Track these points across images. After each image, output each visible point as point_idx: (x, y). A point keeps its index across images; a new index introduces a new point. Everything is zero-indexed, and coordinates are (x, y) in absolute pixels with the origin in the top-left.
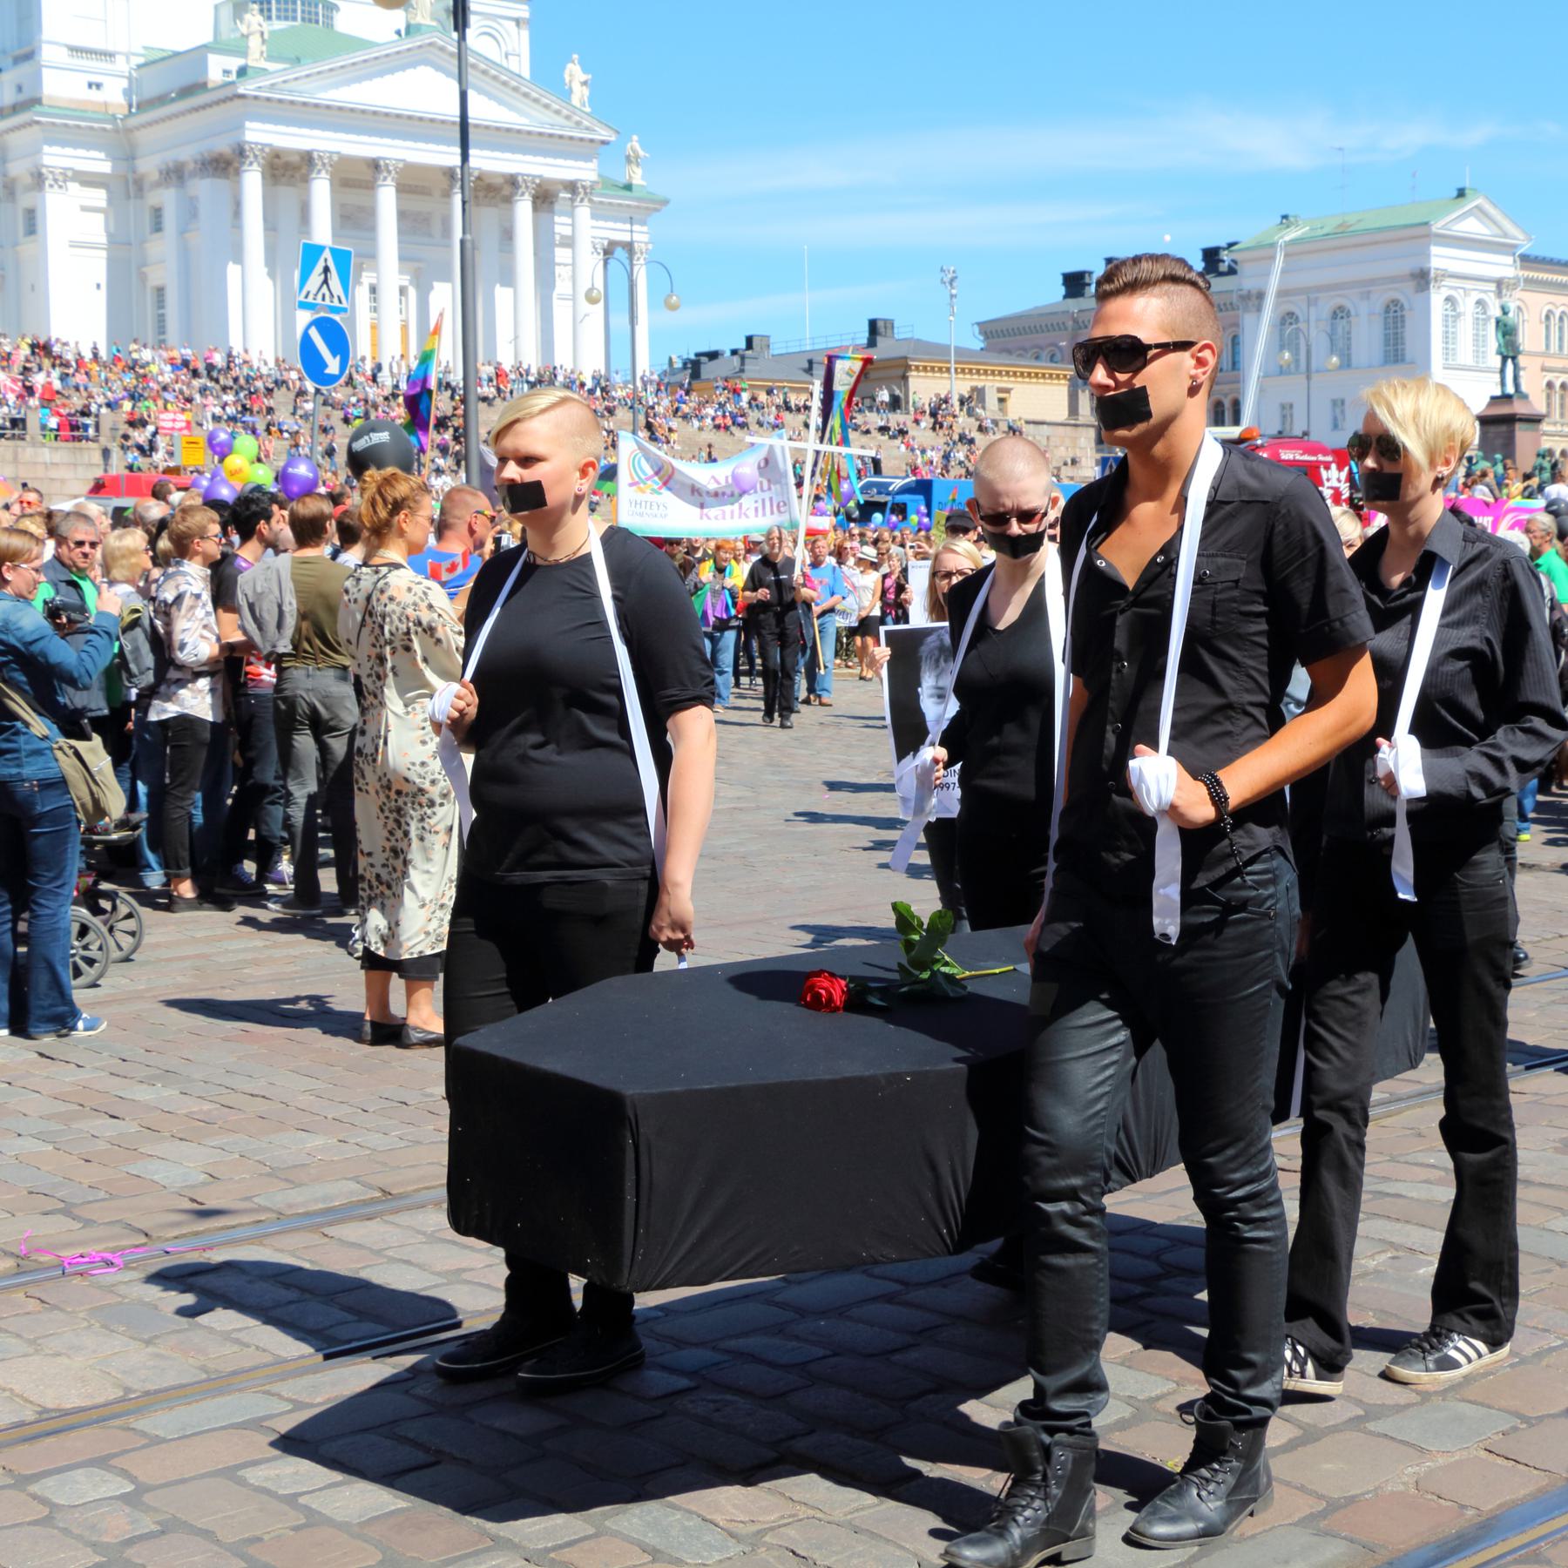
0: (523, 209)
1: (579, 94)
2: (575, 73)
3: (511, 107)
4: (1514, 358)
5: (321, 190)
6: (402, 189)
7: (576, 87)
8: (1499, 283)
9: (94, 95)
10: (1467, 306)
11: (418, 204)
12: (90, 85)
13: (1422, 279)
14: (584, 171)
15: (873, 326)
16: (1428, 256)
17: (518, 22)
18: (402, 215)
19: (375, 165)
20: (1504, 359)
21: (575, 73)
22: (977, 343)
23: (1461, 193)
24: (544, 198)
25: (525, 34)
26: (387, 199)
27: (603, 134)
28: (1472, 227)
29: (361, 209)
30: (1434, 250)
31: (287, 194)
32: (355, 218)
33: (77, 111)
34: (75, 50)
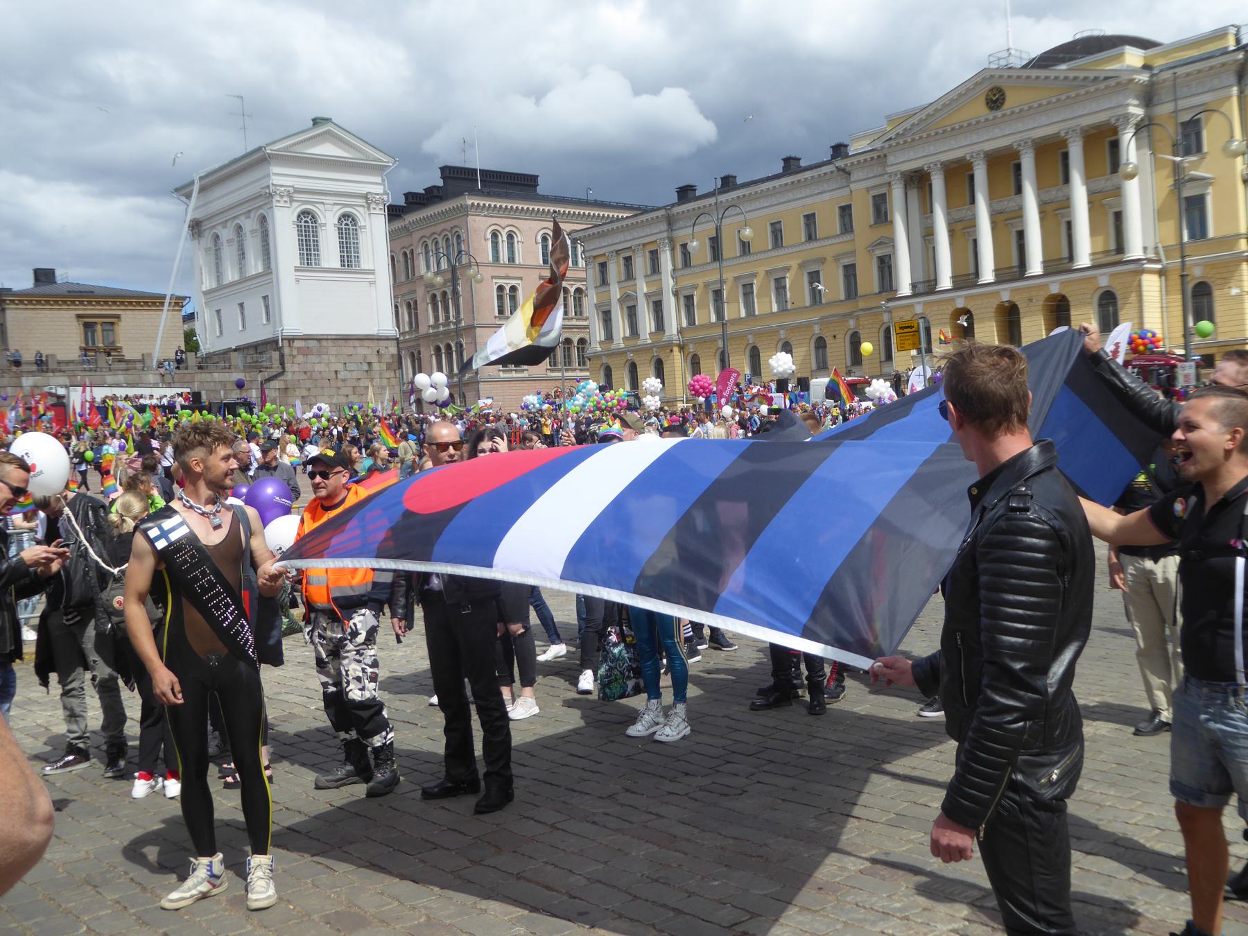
10: (328, 219)
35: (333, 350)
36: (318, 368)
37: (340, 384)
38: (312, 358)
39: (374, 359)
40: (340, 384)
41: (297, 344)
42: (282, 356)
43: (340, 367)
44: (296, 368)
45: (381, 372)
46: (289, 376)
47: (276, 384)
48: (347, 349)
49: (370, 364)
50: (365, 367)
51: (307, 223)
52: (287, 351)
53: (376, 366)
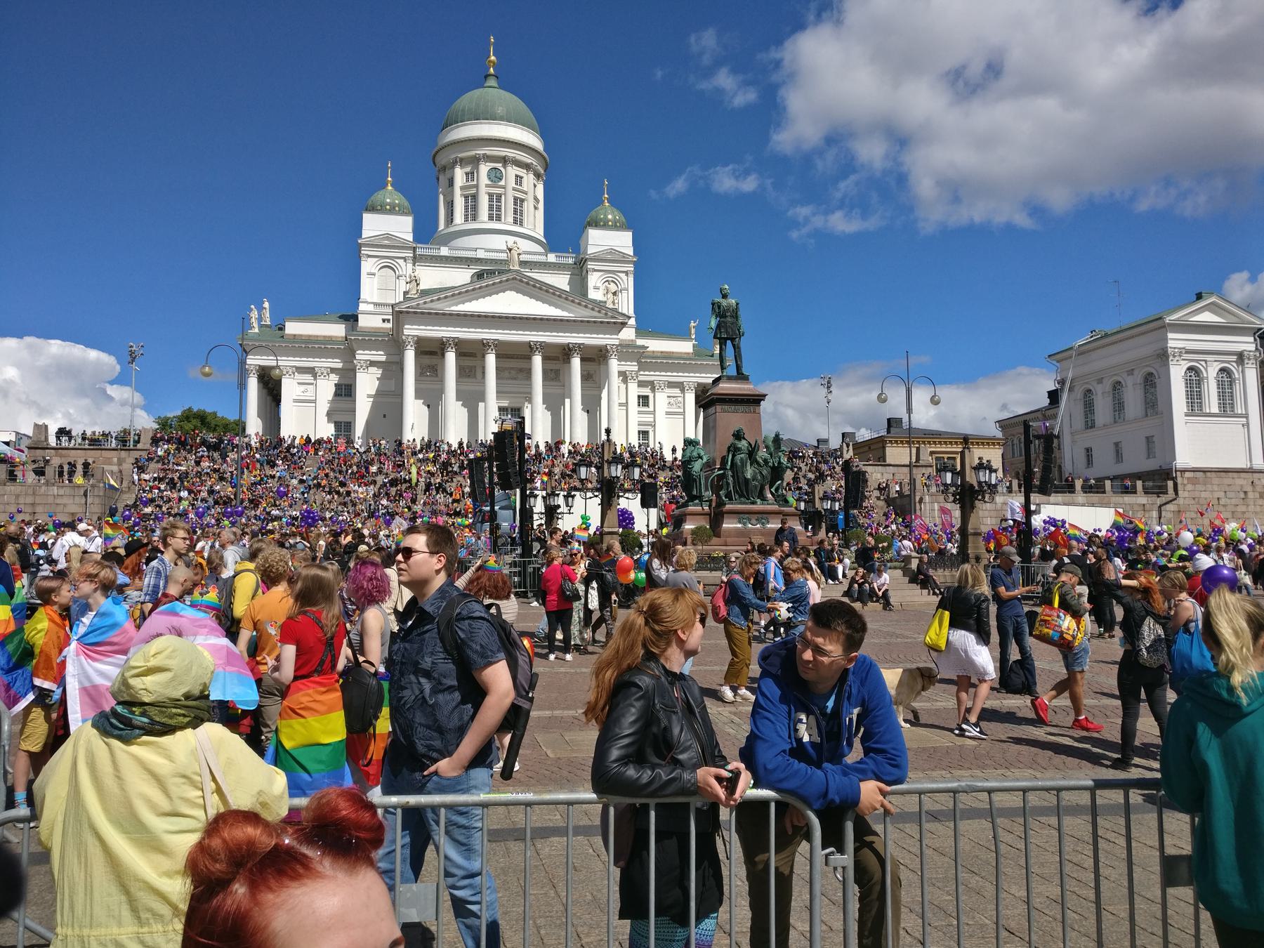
3: (557, 306)
4: (732, 340)
8: (1241, 357)
10: (1211, 373)
12: (384, 321)
13: (1163, 356)
15: (889, 420)
16: (1166, 340)
17: (626, 273)
20: (723, 343)
22: (999, 434)
23: (1199, 297)
25: (631, 279)
26: (491, 359)
28: (1207, 317)
30: (1170, 335)
34: (376, 304)
35: (1216, 481)
36: (1203, 495)
37: (1221, 508)
38: (1199, 487)
39: (1249, 488)
40: (1221, 508)
41: (1187, 475)
42: (1176, 485)
43: (1221, 495)
44: (1186, 494)
45: (1255, 499)
46: (1180, 501)
47: (1170, 507)
48: (1227, 480)
49: (1245, 493)
50: (1242, 495)
51: (1194, 377)
52: (1179, 480)
53: (1251, 495)
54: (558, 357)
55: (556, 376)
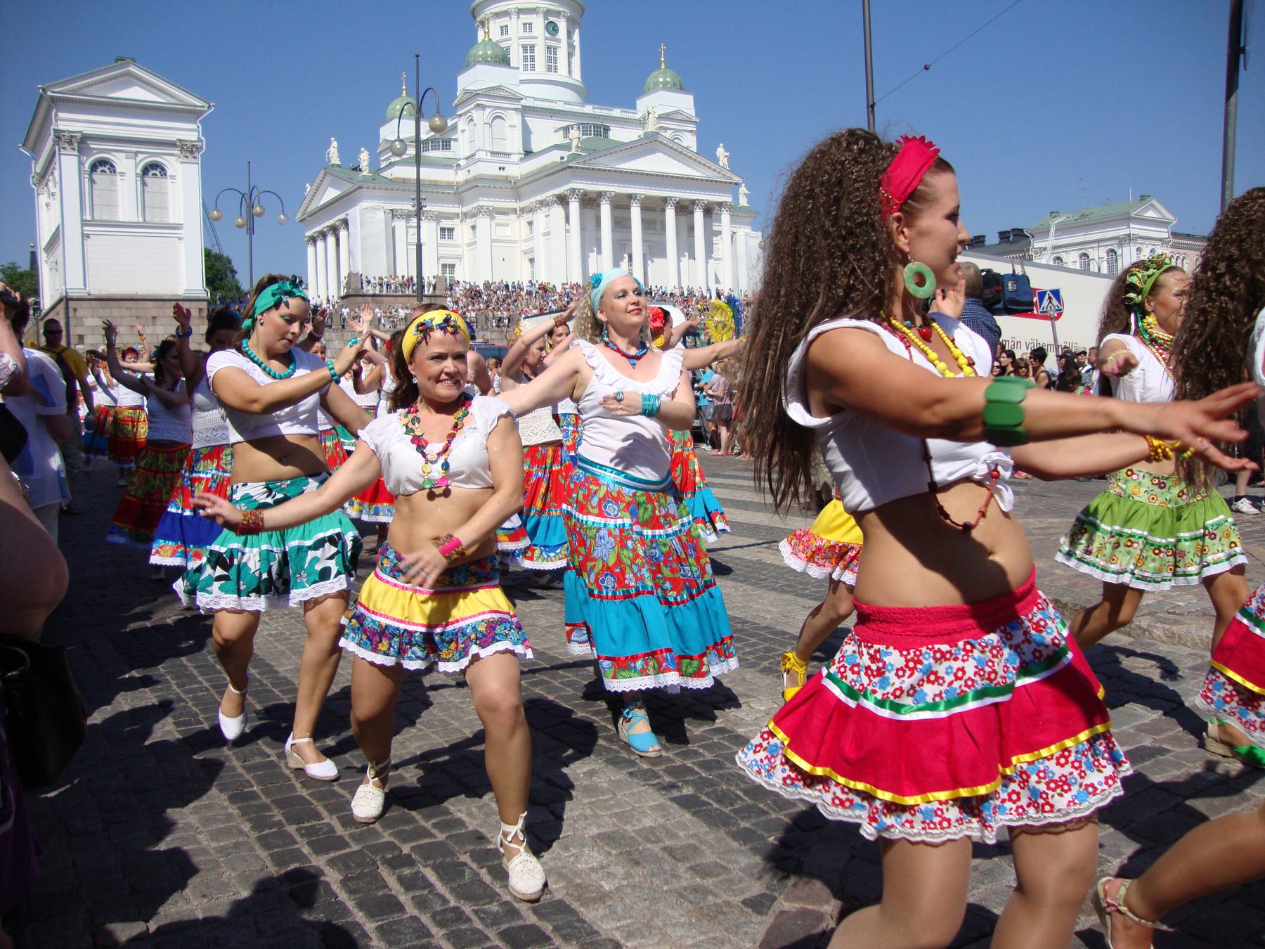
0: (699, 216)
1: (723, 161)
2: (721, 152)
5: (605, 209)
6: (644, 209)
7: (721, 158)
9: (502, 173)
11: (650, 215)
14: (727, 199)
18: (643, 220)
19: (630, 197)
21: (721, 152)
24: (709, 211)
26: (636, 213)
27: (736, 179)
29: (624, 218)
31: (590, 213)
32: (621, 223)
33: (495, 179)
54: (684, 209)
55: (653, 225)
